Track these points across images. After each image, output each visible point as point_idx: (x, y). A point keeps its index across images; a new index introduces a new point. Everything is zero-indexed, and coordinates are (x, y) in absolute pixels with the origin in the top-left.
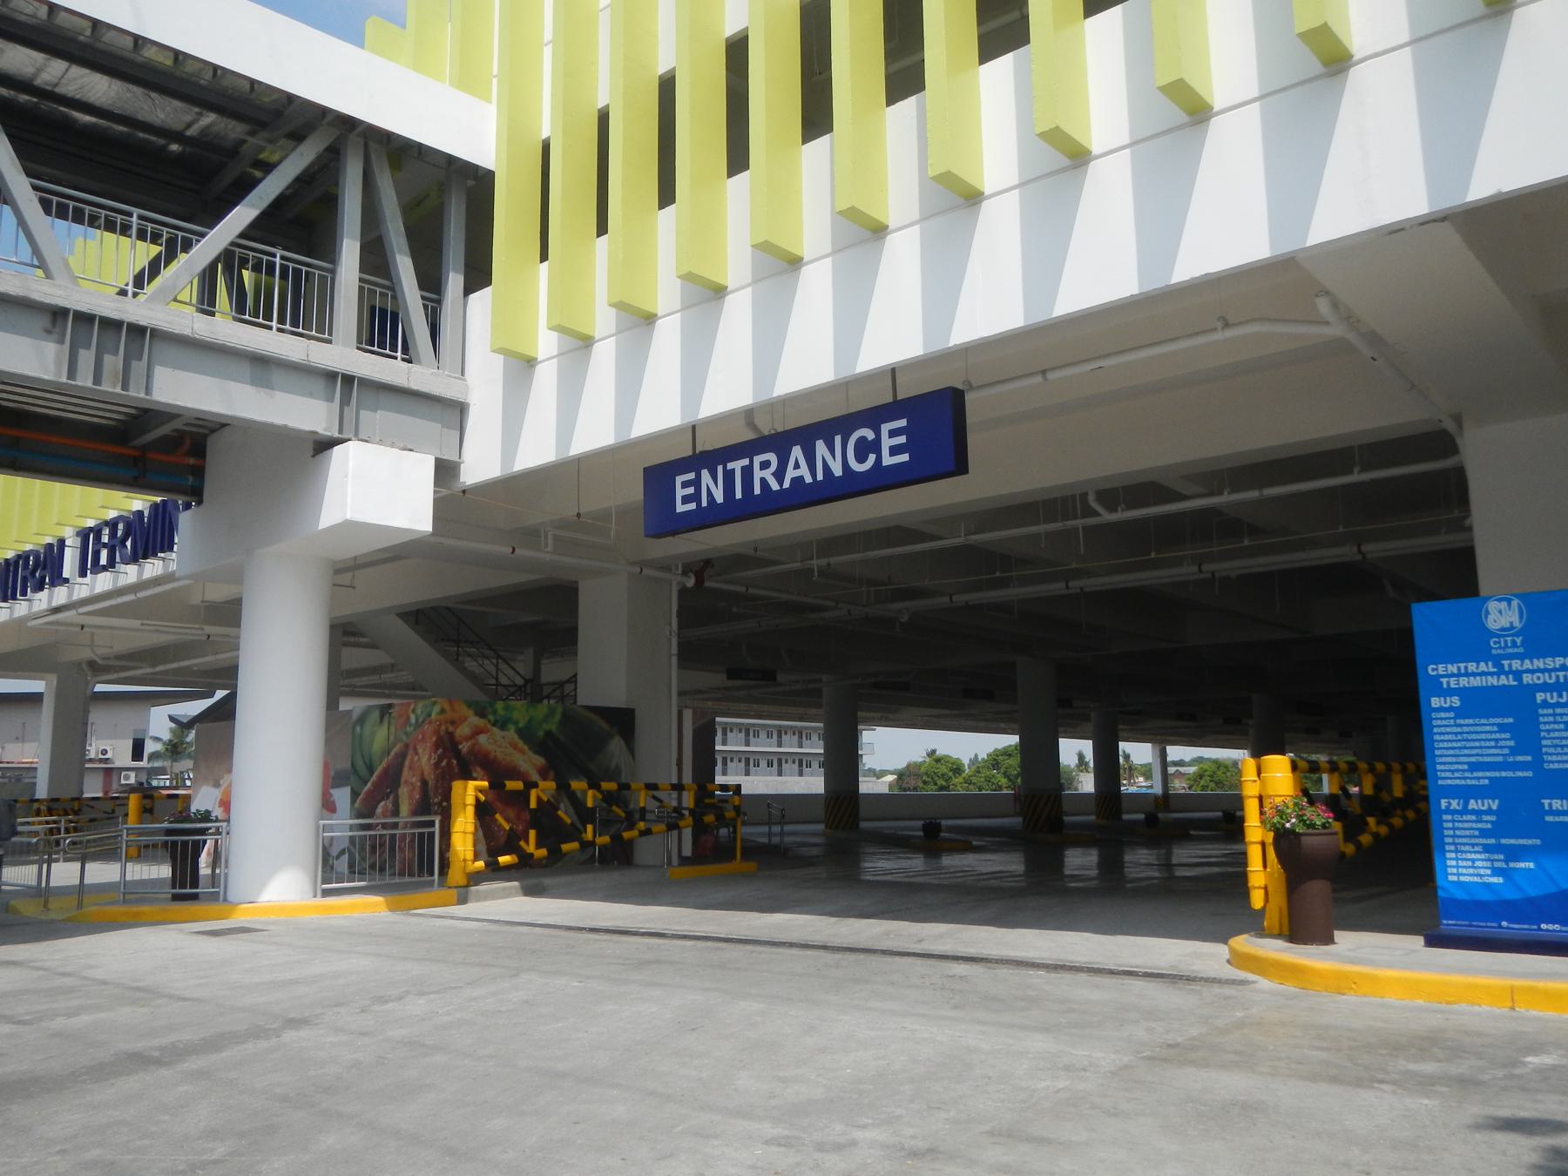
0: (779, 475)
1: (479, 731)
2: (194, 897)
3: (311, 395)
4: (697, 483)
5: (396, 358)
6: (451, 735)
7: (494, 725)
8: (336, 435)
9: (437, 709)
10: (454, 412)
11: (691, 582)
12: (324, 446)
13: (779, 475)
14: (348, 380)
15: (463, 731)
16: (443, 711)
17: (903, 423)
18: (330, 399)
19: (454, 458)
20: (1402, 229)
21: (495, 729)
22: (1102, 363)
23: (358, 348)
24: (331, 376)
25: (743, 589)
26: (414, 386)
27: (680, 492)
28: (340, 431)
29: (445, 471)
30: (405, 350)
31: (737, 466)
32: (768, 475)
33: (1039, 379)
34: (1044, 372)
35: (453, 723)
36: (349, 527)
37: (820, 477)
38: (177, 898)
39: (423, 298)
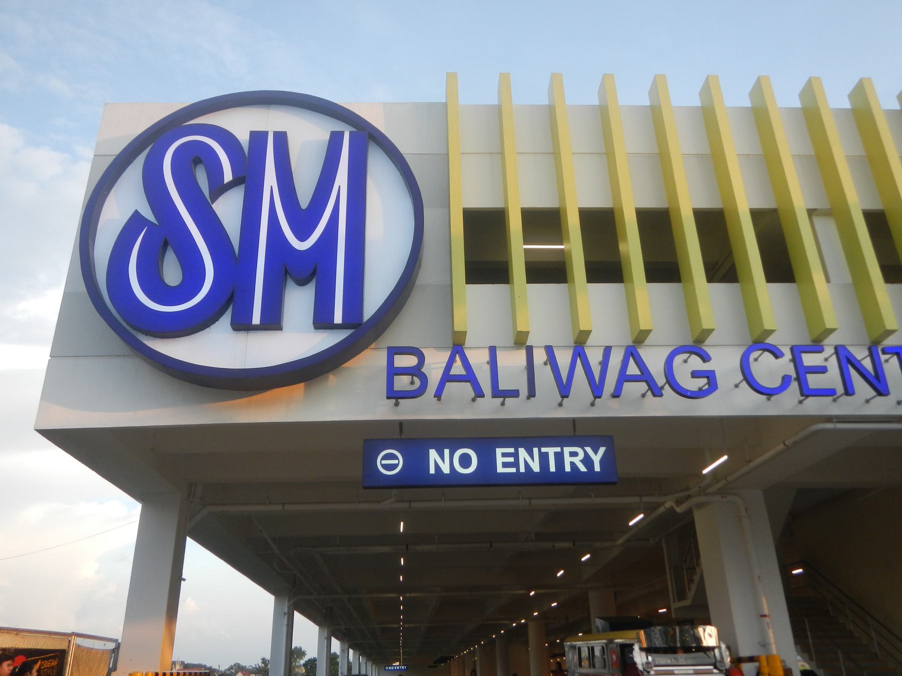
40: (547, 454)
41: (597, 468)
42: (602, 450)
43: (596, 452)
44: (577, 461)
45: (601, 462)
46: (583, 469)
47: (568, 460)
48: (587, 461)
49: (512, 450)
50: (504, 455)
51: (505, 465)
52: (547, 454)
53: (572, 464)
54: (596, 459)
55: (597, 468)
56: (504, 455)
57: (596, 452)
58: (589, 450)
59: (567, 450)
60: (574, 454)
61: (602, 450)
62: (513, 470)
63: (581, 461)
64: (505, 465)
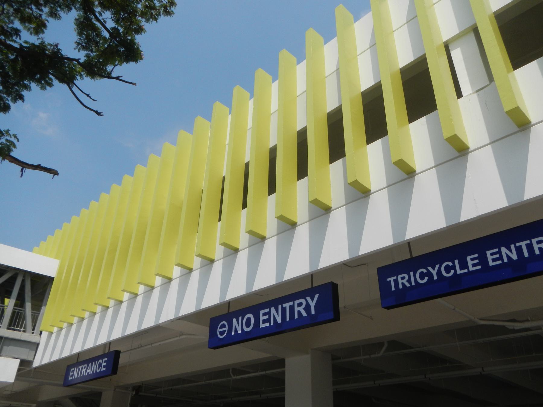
0: (86, 371)
4: (73, 371)
5: (20, 331)
10: (37, 345)
11: (134, 393)
13: (86, 371)
17: (106, 359)
20: (173, 321)
22: (162, 343)
23: (8, 329)
25: (155, 395)
26: (22, 339)
27: (71, 374)
29: (24, 364)
30: (24, 329)
31: (81, 367)
32: (84, 370)
33: (150, 346)
34: (151, 344)
37: (92, 373)
39: (32, 312)
40: (286, 307)
41: (313, 312)
42: (317, 296)
43: (312, 300)
44: (301, 309)
45: (316, 306)
46: (304, 314)
47: (296, 309)
48: (308, 308)
49: (267, 310)
50: (264, 314)
51: (265, 321)
52: (286, 307)
53: (299, 312)
54: (313, 304)
55: (313, 312)
56: (264, 314)
57: (312, 300)
58: (308, 299)
59: (297, 302)
60: (300, 305)
61: (317, 296)
62: (267, 325)
63: (304, 309)
64: (265, 321)
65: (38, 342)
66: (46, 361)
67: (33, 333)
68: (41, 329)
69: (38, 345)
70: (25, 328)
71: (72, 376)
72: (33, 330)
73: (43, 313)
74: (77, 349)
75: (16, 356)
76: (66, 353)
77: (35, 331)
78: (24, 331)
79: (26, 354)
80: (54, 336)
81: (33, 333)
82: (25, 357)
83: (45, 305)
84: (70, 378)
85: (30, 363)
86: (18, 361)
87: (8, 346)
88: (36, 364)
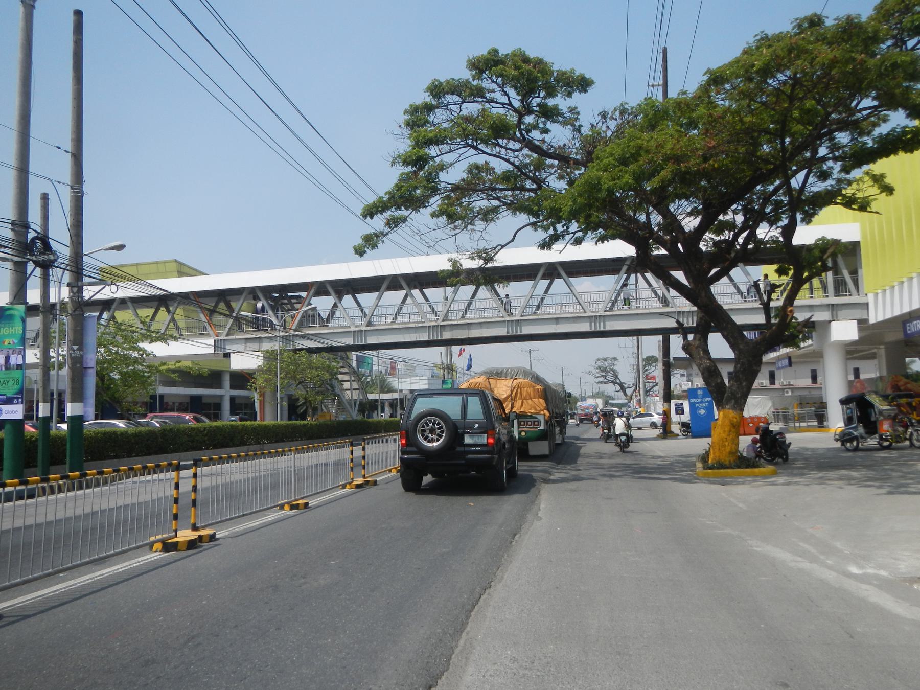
1: (906, 383)
2: (823, 427)
3: (824, 311)
4: (909, 326)
5: (846, 295)
6: (897, 385)
7: (912, 381)
8: (831, 319)
9: (891, 378)
12: (830, 321)
14: (833, 305)
15: (901, 383)
16: (893, 378)
18: (829, 311)
19: (867, 318)
21: (914, 384)
23: (836, 296)
24: (828, 305)
27: (908, 328)
28: (832, 317)
29: (862, 323)
35: (897, 381)
36: (835, 341)
38: (819, 427)
65: (866, 302)
66: (881, 318)
67: (859, 295)
68: (865, 292)
69: (867, 304)
70: (849, 292)
71: (909, 330)
72: (858, 291)
73: (862, 276)
74: (906, 310)
75: (851, 318)
76: (897, 313)
77: (860, 293)
78: (850, 295)
79: (861, 315)
80: (880, 296)
81: (859, 295)
82: (859, 317)
83: (861, 268)
84: (909, 332)
85: (866, 321)
86: (856, 321)
87: (841, 310)
88: (872, 320)
